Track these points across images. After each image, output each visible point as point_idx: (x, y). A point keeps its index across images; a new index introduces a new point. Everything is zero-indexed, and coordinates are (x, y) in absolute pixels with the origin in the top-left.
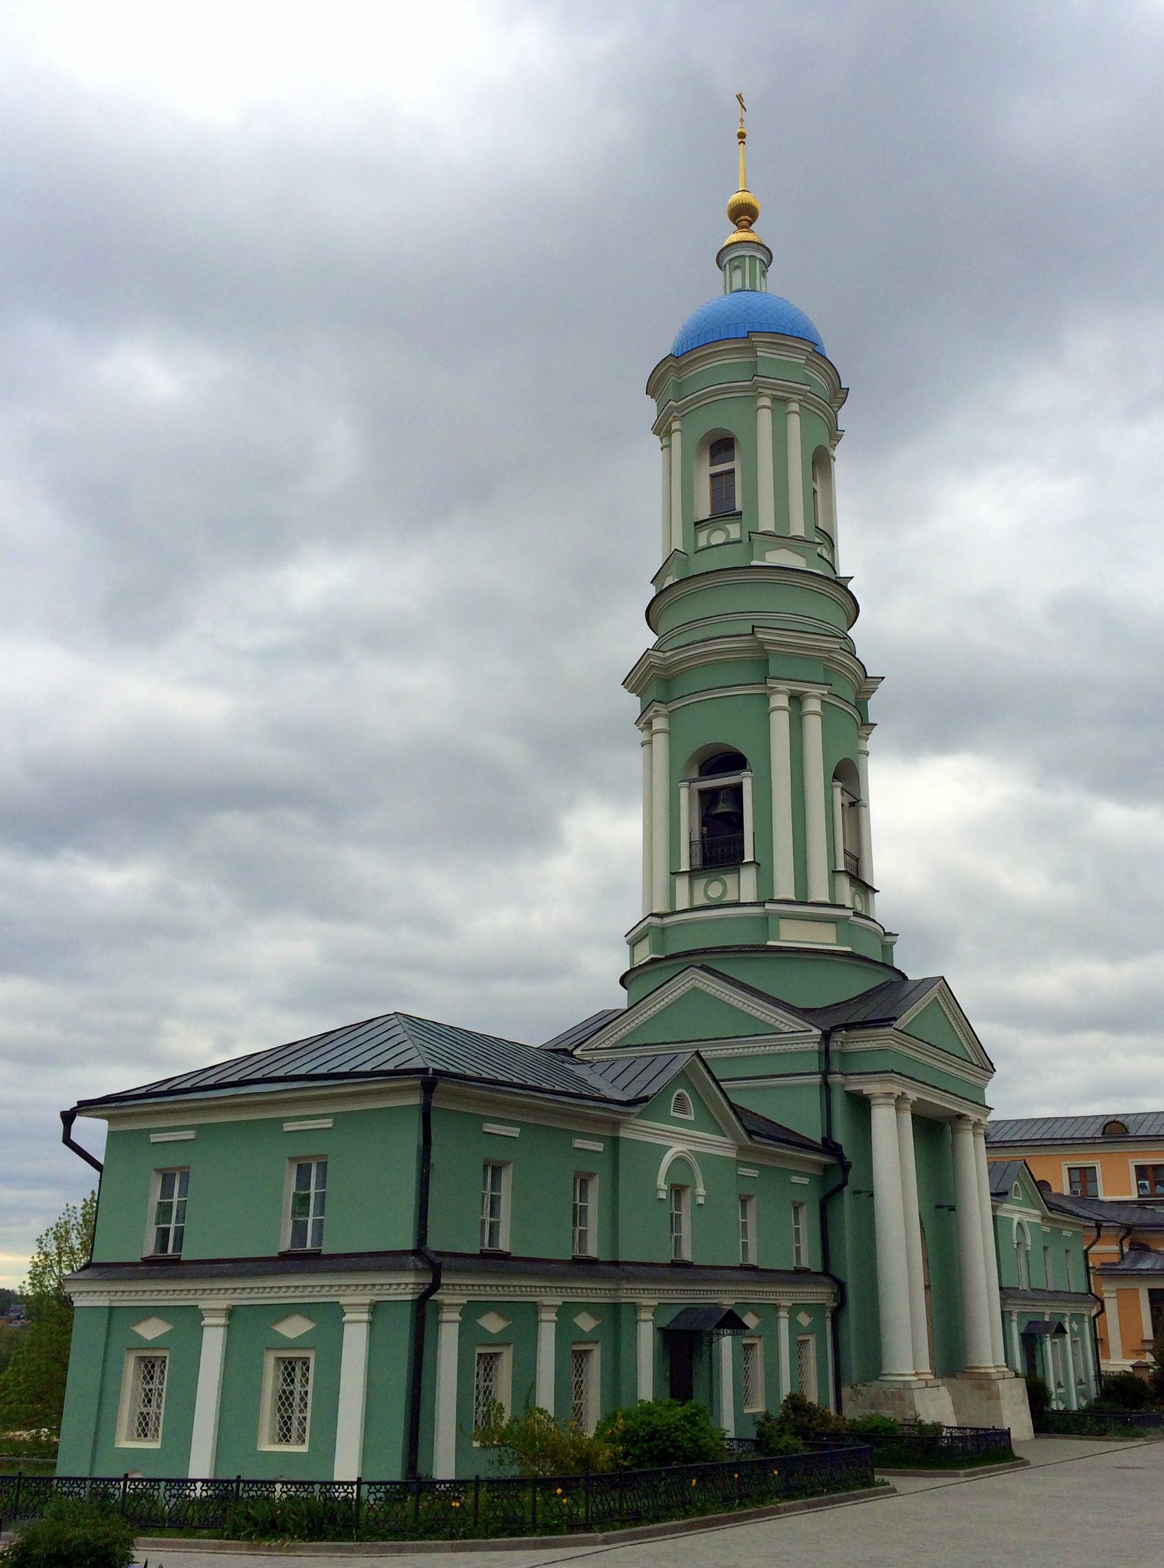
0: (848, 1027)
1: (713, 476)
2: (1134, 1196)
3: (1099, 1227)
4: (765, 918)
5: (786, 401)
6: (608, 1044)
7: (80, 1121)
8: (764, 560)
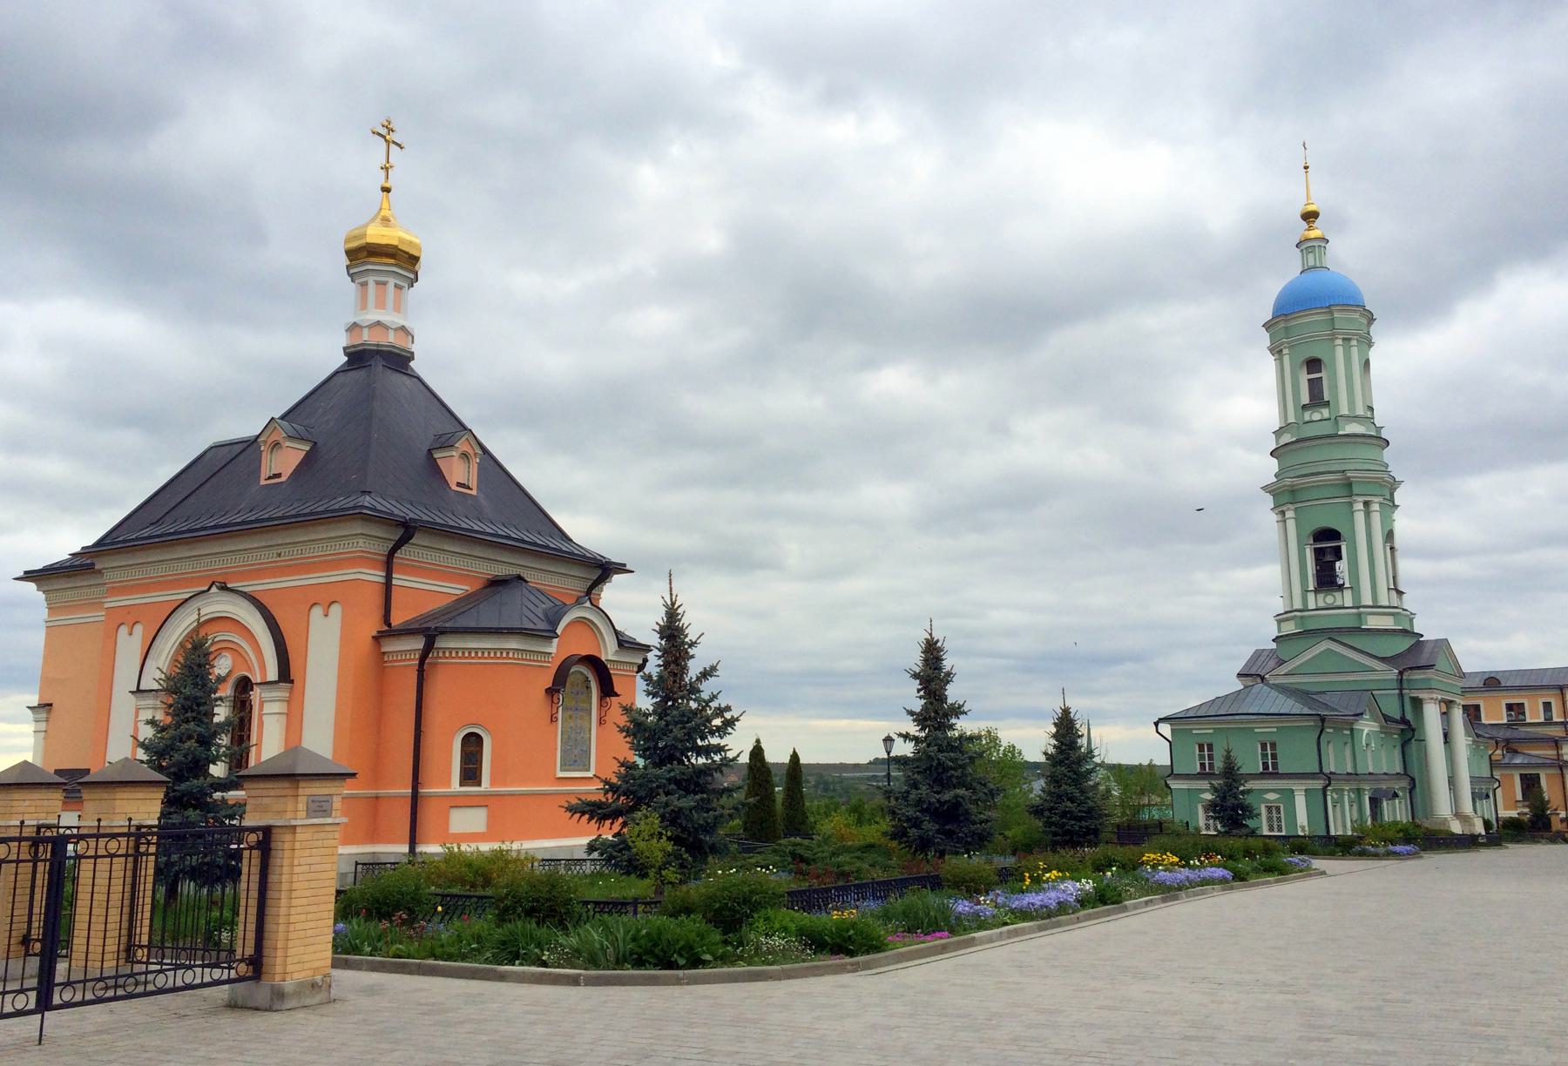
0: (1411, 669)
2: (1505, 721)
3: (1497, 743)
4: (1359, 615)
5: (1349, 340)
6: (1282, 673)
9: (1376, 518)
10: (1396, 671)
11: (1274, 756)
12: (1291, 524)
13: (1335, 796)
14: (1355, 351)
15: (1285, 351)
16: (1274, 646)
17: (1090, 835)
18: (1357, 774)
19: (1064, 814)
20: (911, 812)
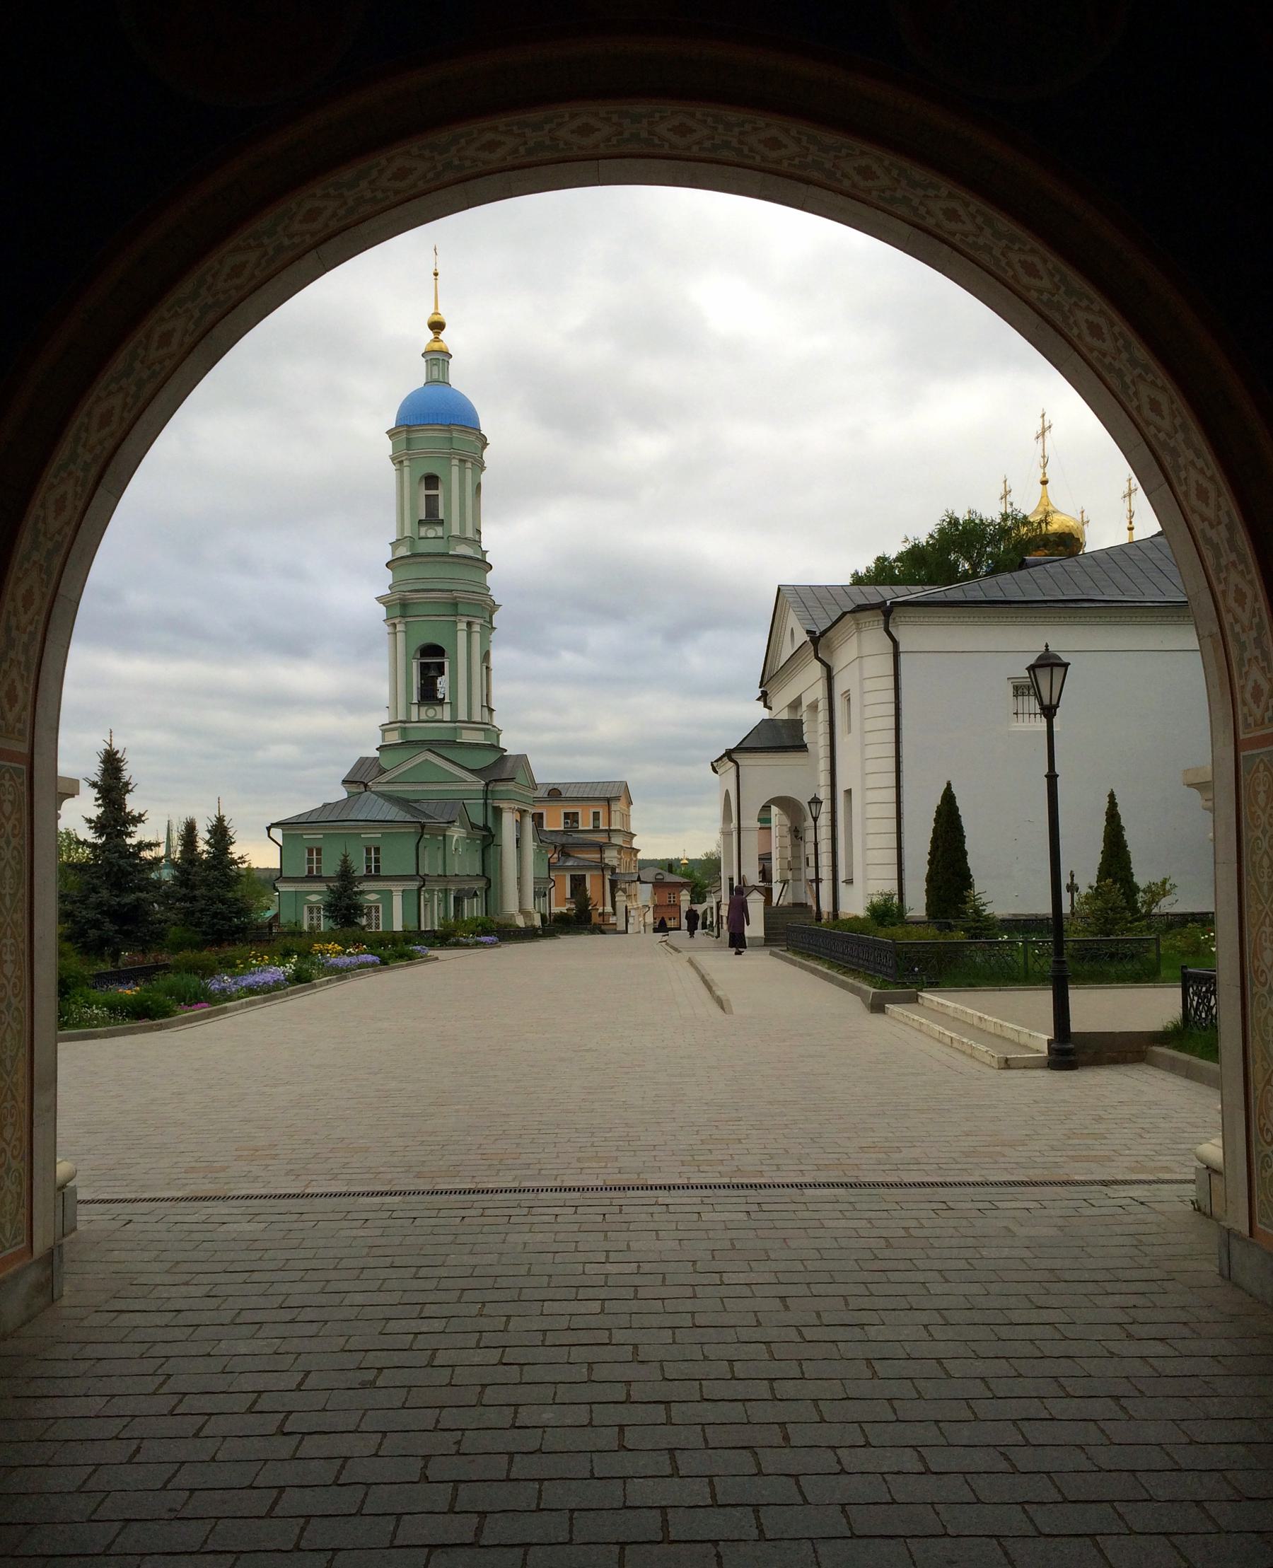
0: (496, 781)
1: (427, 496)
2: (562, 828)
3: (555, 848)
4: (455, 728)
7: (272, 830)
8: (454, 550)
9: (476, 638)
10: (483, 782)
11: (377, 860)
12: (400, 636)
13: (427, 896)
14: (469, 473)
15: (406, 463)
16: (377, 754)
17: (239, 933)
18: (445, 876)
19: (215, 915)
20: (91, 914)
